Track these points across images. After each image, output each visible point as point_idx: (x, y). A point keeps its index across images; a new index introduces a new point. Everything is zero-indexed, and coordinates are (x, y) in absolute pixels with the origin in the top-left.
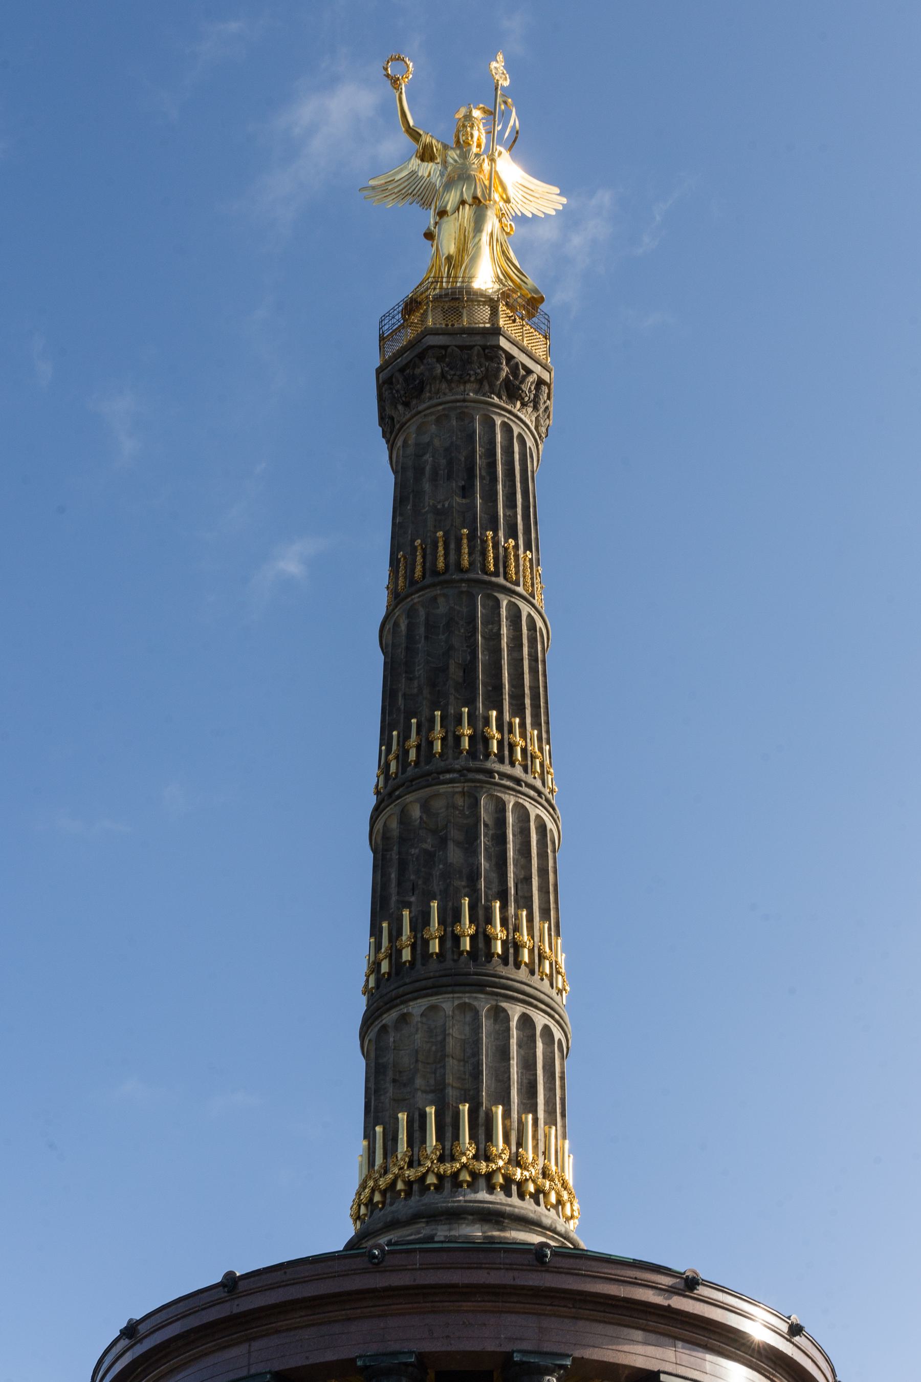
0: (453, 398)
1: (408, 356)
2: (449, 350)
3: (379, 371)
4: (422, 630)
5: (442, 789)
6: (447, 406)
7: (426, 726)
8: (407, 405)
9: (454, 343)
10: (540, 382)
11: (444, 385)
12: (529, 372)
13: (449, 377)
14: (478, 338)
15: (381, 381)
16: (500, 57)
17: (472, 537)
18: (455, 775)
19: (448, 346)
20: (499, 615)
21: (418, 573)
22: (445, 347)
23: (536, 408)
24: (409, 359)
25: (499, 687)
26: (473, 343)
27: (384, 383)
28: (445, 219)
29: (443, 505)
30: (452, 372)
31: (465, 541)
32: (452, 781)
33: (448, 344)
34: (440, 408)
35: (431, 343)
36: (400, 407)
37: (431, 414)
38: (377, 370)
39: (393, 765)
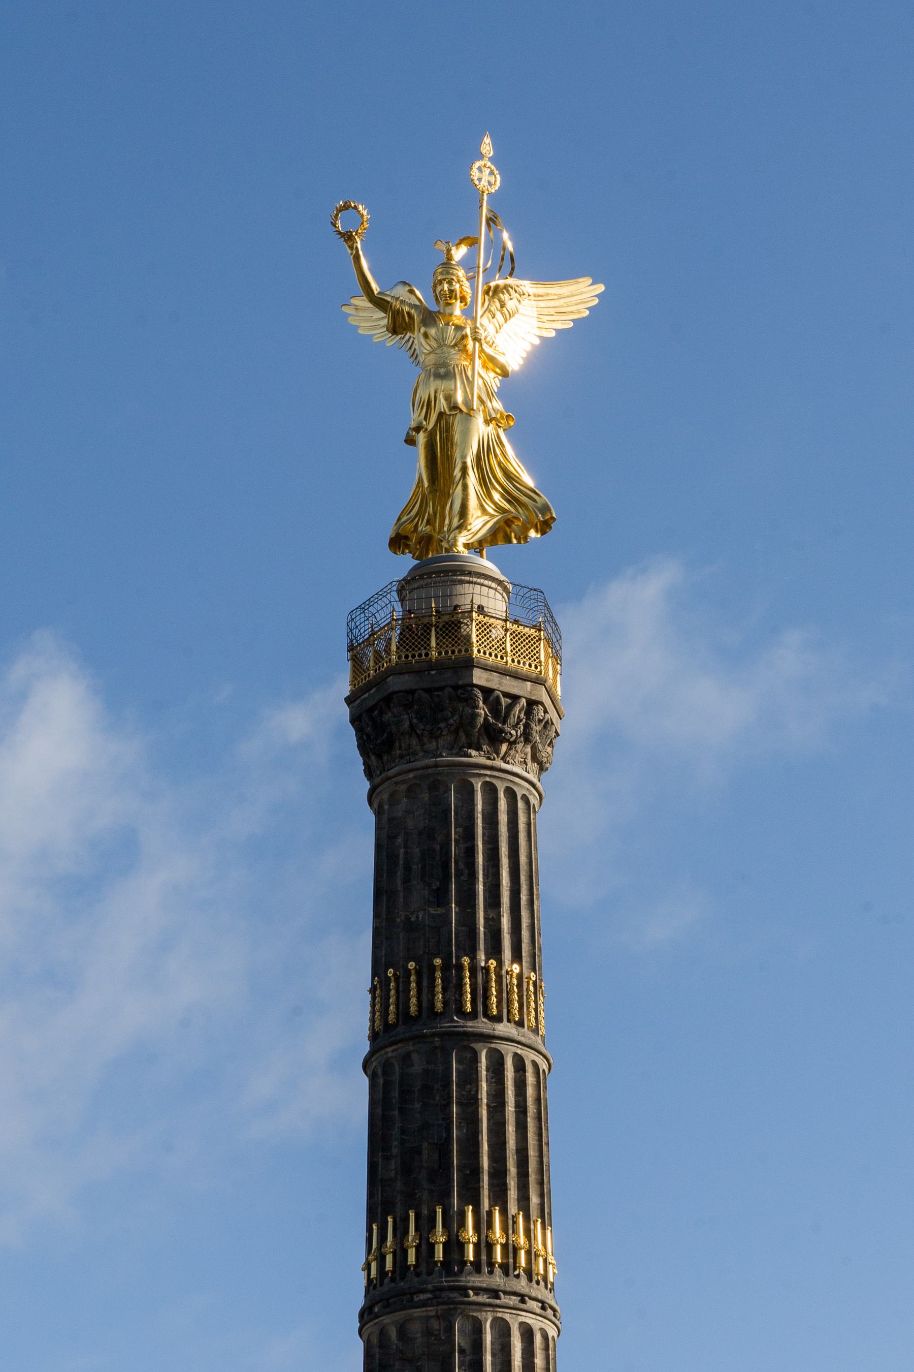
2: (416, 695)
3: (349, 701)
4: (396, 1094)
5: (417, 1312)
6: (419, 773)
7: (401, 1232)
8: (379, 756)
10: (532, 704)
12: (515, 698)
16: (487, 147)
17: (446, 968)
18: (429, 1295)
19: (416, 690)
20: (477, 1072)
21: (391, 1018)
22: (412, 692)
25: (476, 1171)
26: (443, 684)
29: (417, 917)
30: (422, 727)
31: (438, 974)
32: (424, 1304)
33: (414, 687)
34: (411, 775)
37: (403, 782)
39: (374, 1265)
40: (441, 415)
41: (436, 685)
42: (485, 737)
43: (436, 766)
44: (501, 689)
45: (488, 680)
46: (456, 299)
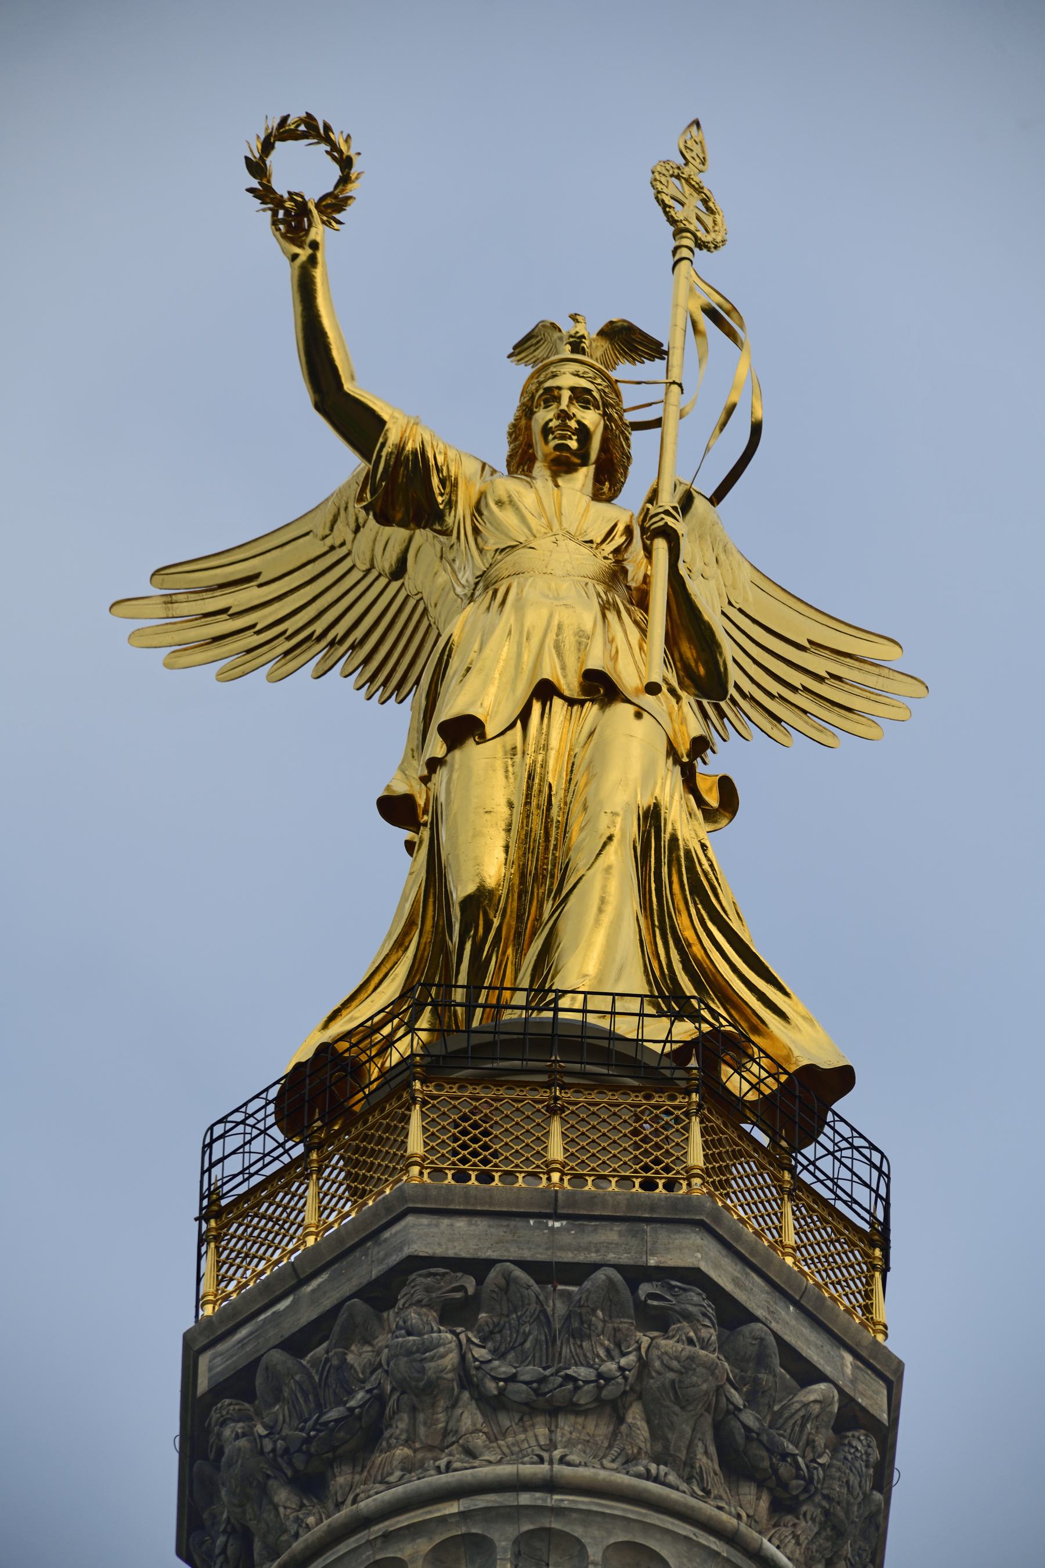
0: (505, 1470)
1: (321, 1294)
8: (312, 1486)
9: (515, 1253)
10: (850, 1417)
11: (469, 1417)
13: (491, 1387)
14: (611, 1234)
15: (203, 1385)
19: (491, 1263)
22: (479, 1267)
23: (833, 1527)
24: (327, 1304)
26: (594, 1257)
27: (219, 1390)
28: (472, 749)
30: (504, 1369)
33: (490, 1254)
34: (452, 1508)
35: (420, 1248)
36: (282, 1495)
37: (414, 1531)
38: (188, 1339)
40: (545, 691)
41: (568, 1257)
42: (712, 1449)
43: (550, 1486)
44: (774, 1325)
45: (736, 1281)
46: (585, 463)
